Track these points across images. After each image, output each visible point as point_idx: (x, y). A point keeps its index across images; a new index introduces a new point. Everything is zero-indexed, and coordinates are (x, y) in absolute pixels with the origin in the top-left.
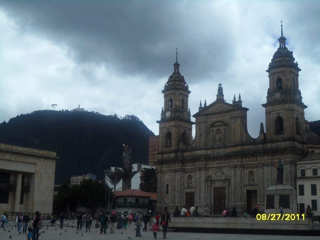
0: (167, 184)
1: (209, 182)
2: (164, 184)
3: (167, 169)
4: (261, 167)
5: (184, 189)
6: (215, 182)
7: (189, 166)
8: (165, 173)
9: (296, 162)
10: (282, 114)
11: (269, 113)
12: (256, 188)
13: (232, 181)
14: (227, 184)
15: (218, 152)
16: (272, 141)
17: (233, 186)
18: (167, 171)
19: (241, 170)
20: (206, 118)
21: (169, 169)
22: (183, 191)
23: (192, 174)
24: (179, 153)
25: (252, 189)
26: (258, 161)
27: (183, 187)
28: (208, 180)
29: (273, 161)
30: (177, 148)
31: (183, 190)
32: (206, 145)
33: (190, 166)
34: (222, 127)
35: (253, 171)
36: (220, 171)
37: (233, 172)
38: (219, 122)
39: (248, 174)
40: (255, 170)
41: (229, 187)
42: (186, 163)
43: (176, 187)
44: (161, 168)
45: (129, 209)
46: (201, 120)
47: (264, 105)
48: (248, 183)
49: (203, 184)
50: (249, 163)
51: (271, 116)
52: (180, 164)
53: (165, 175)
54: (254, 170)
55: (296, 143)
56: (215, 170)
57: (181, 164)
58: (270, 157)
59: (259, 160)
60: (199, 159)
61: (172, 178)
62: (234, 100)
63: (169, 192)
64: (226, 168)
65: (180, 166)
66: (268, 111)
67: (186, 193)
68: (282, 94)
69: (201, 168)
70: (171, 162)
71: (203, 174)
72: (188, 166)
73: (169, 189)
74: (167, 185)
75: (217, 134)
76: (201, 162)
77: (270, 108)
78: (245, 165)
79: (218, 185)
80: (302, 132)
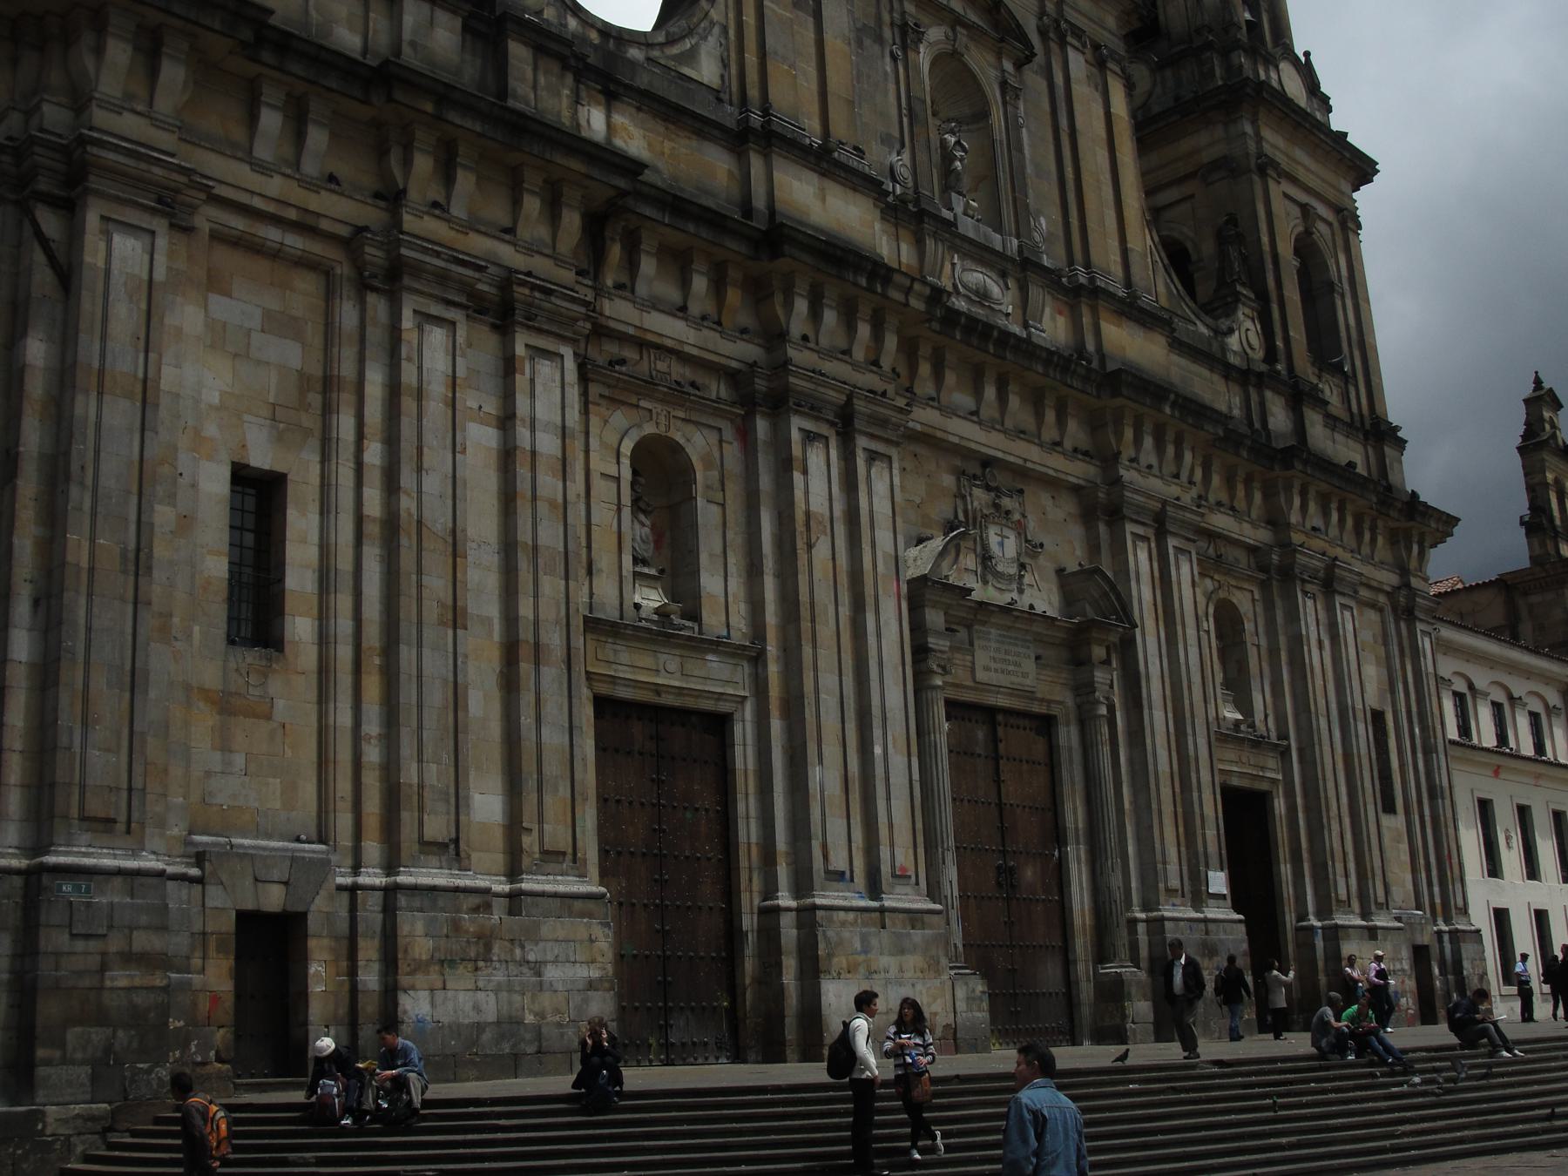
0: (261, 458)
3: (275, 185)
4: (1309, 587)
8: (225, 258)
10: (1321, 226)
11: (1275, 176)
15: (983, 295)
17: (1158, 715)
18: (273, 234)
23: (697, 444)
24: (518, 51)
33: (681, 311)
37: (1143, 556)
50: (1221, 521)
53: (215, 283)
56: (948, 480)
61: (420, 395)
63: (300, 627)
64: (1045, 499)
69: (860, 405)
71: (881, 487)
73: (299, 578)
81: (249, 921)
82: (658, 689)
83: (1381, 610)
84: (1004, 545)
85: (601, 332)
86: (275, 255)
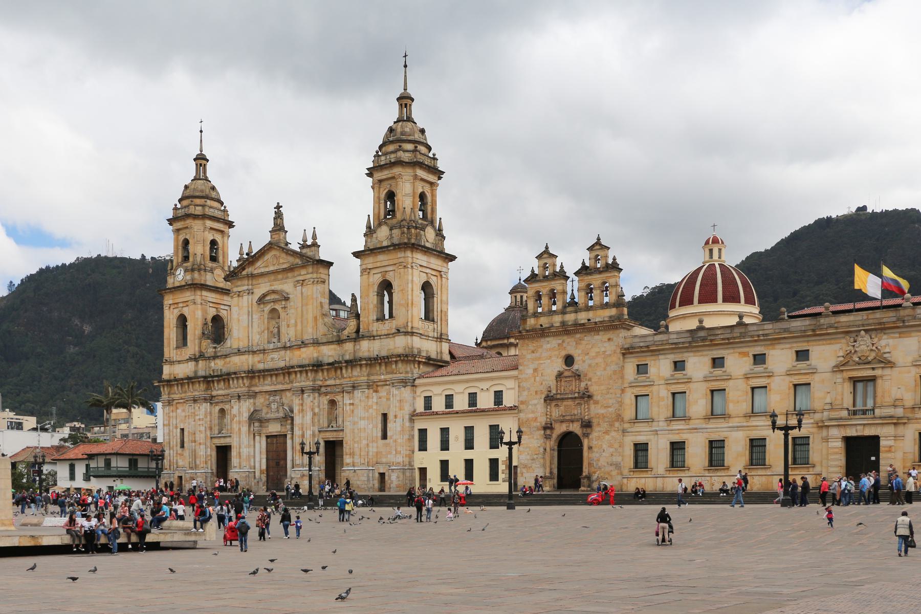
1: (257, 424)
2: (176, 428)
3: (178, 396)
5: (211, 438)
6: (267, 424)
7: (219, 390)
8: (178, 405)
9: (415, 380)
10: (391, 273)
12: (341, 435)
13: (297, 420)
14: (289, 427)
16: (372, 337)
18: (180, 401)
19: (314, 398)
20: (250, 283)
21: (183, 395)
22: (211, 442)
23: (227, 407)
25: (333, 438)
26: (343, 377)
27: (211, 435)
28: (254, 418)
29: (372, 378)
30: (197, 349)
31: (209, 440)
32: (250, 344)
34: (280, 303)
35: (336, 401)
36: (274, 401)
38: (274, 292)
39: (326, 407)
40: (338, 398)
41: (293, 434)
42: (213, 381)
43: (197, 435)
44: (169, 394)
45: (114, 481)
46: (240, 289)
47: (357, 254)
48: (326, 425)
49: (245, 429)
50: (329, 382)
51: (371, 280)
52: (202, 385)
53: (177, 408)
54: (337, 397)
55: (416, 339)
56: (267, 397)
57: (205, 385)
58: (364, 369)
59: (345, 376)
60: (235, 373)
62: (302, 243)
63: (185, 445)
65: (203, 390)
66: (364, 267)
67: (217, 447)
68: (391, 229)
69: (240, 394)
70: (184, 381)
72: (218, 390)
74: (182, 430)
75: (272, 318)
76: (241, 381)
77: (370, 261)
78: (321, 386)
79: (274, 428)
80: (439, 313)
81: (179, 477)
82: (222, 444)
83: (390, 385)
84: (274, 406)
85: (212, 397)
86: (181, 403)
